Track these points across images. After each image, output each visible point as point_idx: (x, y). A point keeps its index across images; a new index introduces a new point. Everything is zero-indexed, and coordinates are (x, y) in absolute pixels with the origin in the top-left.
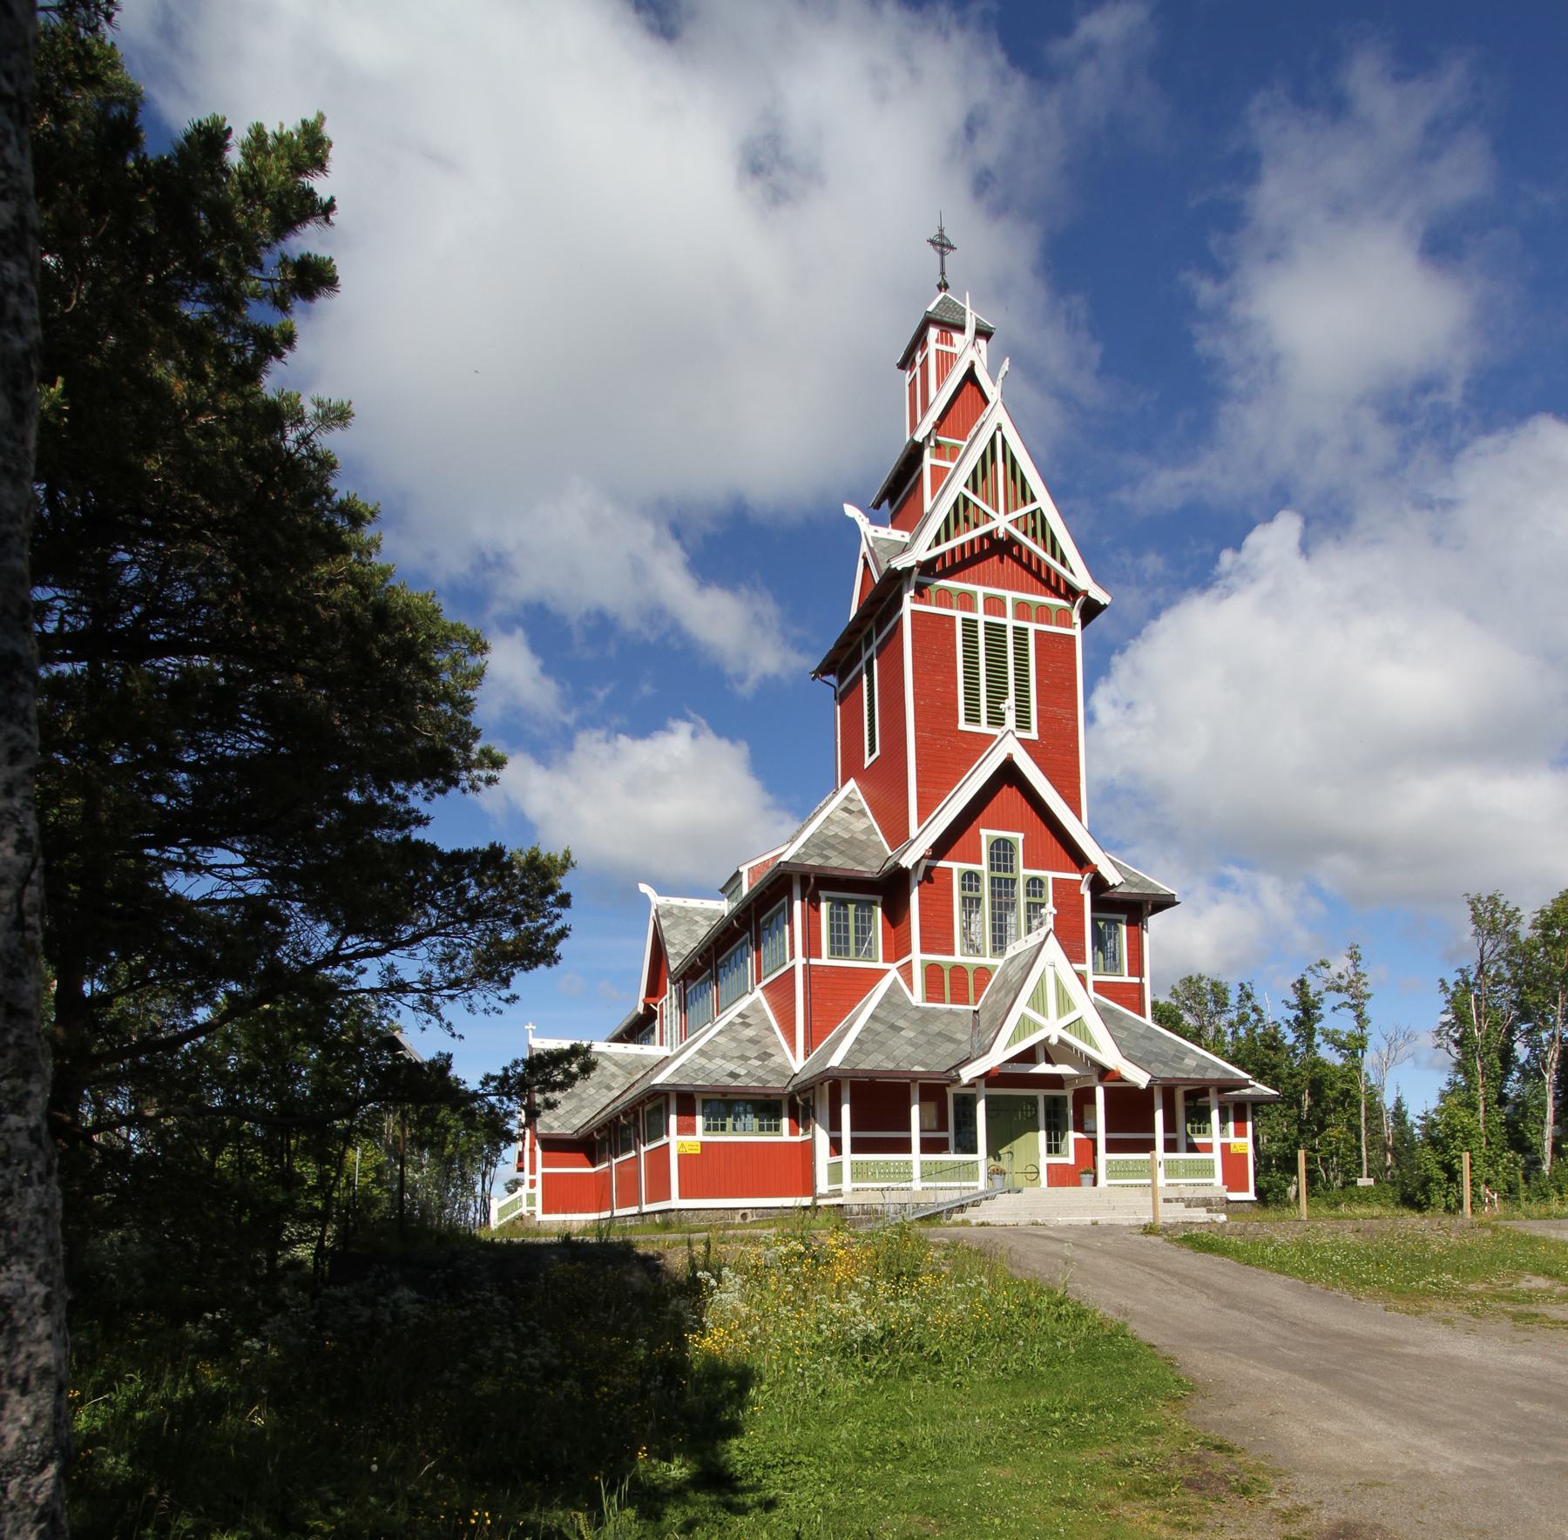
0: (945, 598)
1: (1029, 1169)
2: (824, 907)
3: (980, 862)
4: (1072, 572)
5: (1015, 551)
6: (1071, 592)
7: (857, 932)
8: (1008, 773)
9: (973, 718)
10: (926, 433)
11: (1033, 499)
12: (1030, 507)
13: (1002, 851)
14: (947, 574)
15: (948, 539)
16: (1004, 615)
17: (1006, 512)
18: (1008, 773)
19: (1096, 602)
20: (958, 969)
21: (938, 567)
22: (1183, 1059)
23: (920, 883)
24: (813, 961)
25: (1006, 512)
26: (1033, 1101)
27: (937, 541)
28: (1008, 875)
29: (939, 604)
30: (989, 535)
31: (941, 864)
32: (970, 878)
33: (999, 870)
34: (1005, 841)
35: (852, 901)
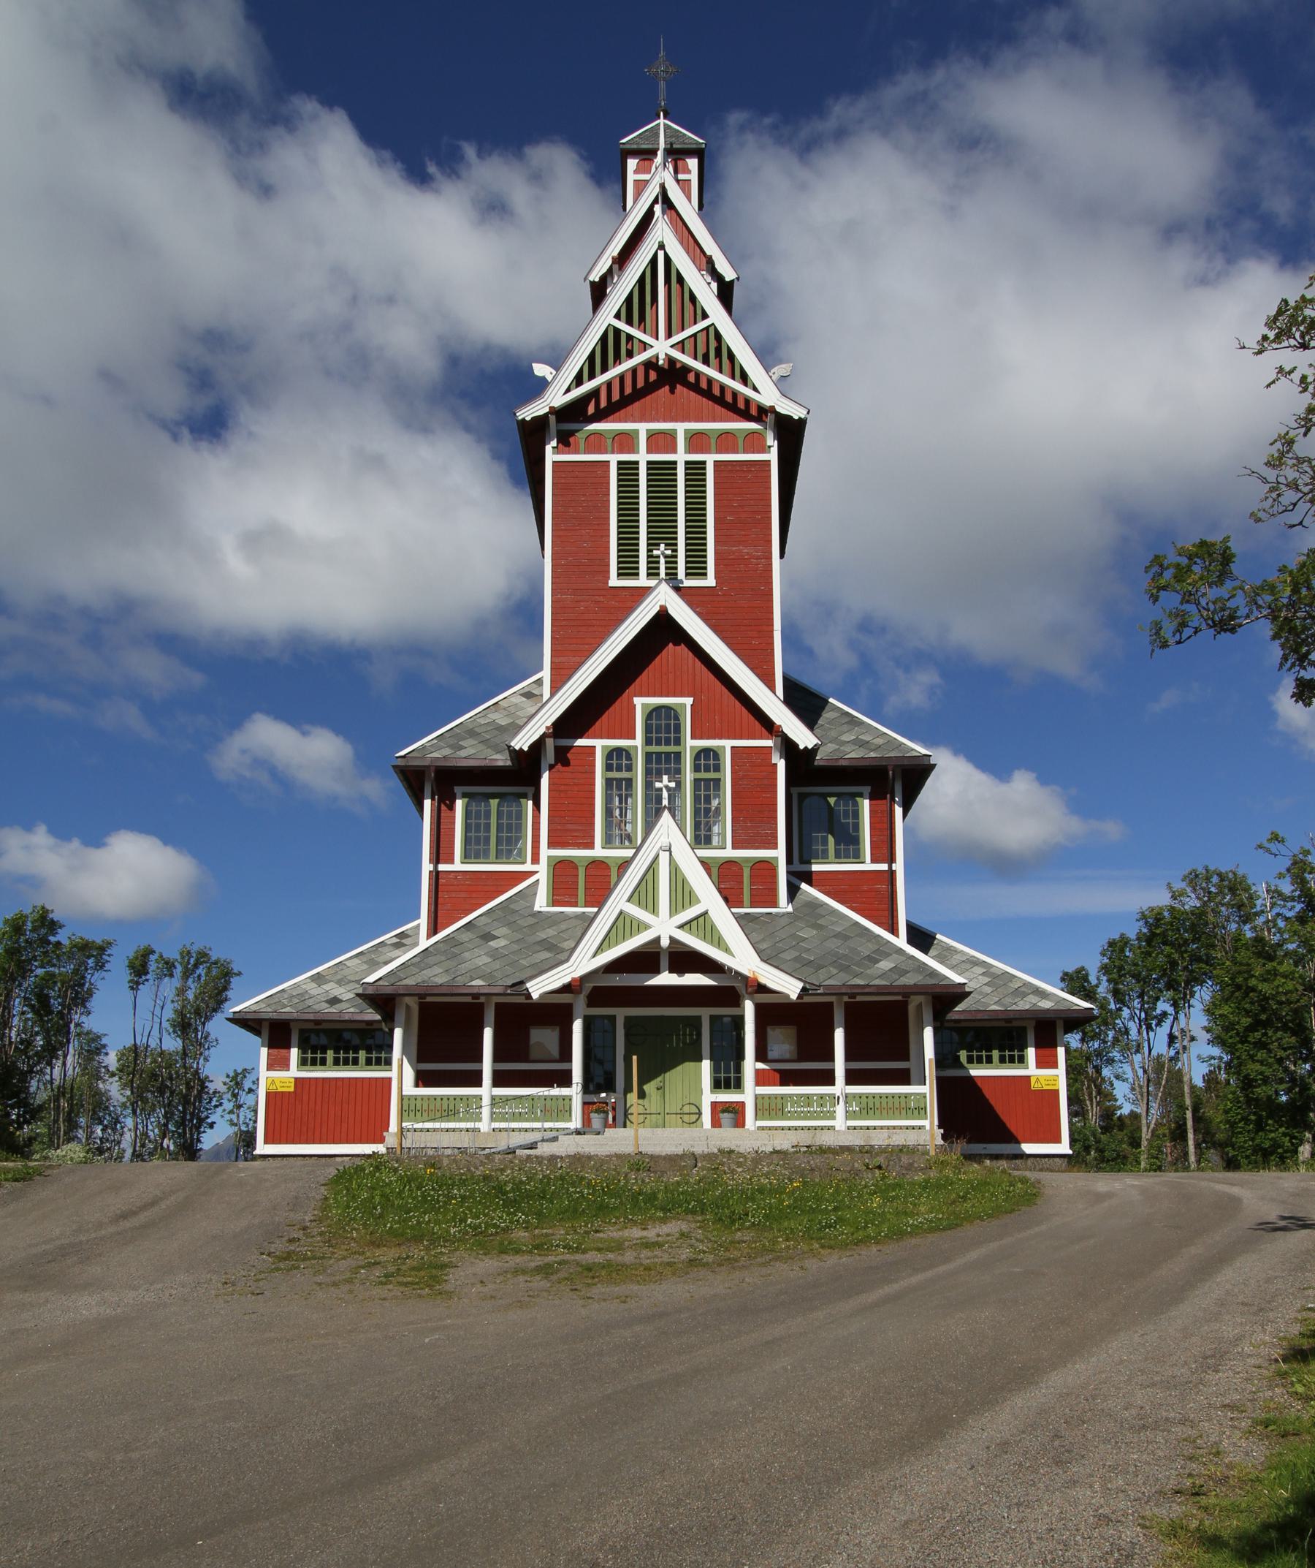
0: (597, 443)
1: (686, 1109)
2: (459, 804)
3: (634, 738)
4: (755, 389)
5: (691, 378)
6: (762, 413)
7: (488, 827)
8: (663, 628)
9: (628, 569)
10: (604, 270)
11: (705, 316)
12: (702, 325)
13: (664, 725)
14: (600, 416)
15: (592, 376)
16: (674, 451)
17: (669, 335)
18: (663, 628)
19: (789, 418)
20: (598, 866)
21: (591, 410)
22: (877, 961)
23: (551, 767)
24: (442, 867)
25: (669, 335)
26: (695, 1023)
27: (579, 380)
28: (672, 749)
29: (588, 451)
30: (650, 365)
31: (580, 742)
32: (618, 758)
33: (659, 743)
34: (668, 708)
35: (494, 796)
